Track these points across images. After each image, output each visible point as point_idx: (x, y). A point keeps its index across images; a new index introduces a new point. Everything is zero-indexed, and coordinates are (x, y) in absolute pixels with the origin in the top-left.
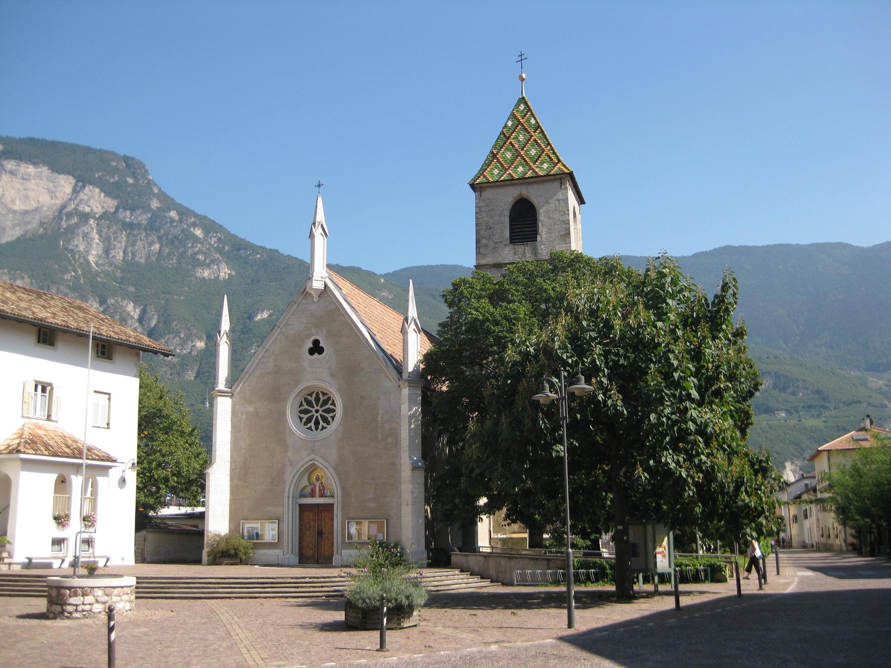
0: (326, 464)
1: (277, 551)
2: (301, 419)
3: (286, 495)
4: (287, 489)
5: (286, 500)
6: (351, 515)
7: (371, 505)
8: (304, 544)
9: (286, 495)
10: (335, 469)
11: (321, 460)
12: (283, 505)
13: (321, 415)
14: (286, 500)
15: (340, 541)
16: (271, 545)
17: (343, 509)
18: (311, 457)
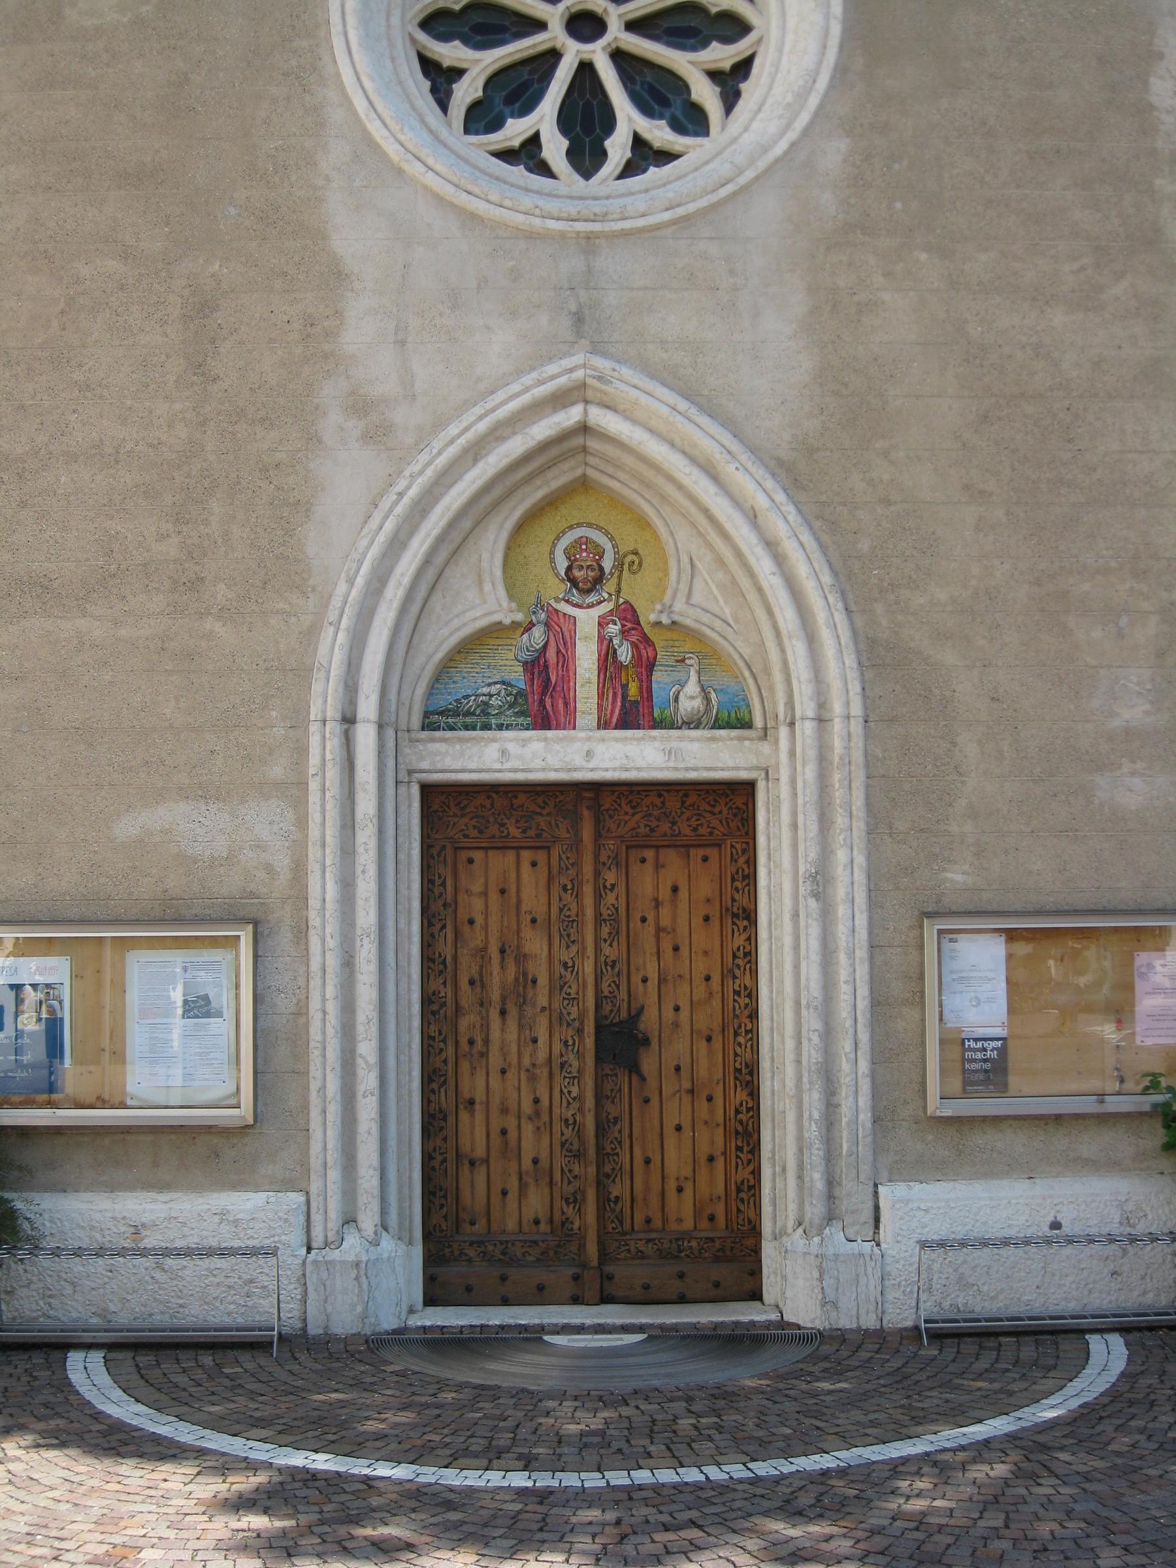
0: (709, 438)
1: (247, 1210)
2: (441, 78)
3: (324, 698)
4: (332, 649)
5: (321, 746)
6: (957, 876)
7: (1132, 789)
8: (474, 1133)
9: (324, 698)
10: (794, 474)
11: (660, 402)
12: (294, 791)
13: (619, 56)
14: (321, 746)
15: (856, 1105)
16: (191, 1149)
17: (878, 825)
18: (560, 372)
